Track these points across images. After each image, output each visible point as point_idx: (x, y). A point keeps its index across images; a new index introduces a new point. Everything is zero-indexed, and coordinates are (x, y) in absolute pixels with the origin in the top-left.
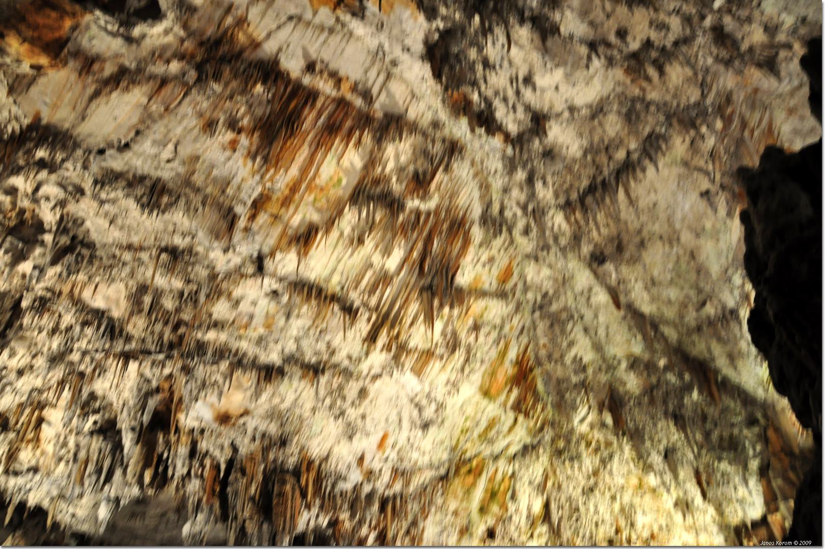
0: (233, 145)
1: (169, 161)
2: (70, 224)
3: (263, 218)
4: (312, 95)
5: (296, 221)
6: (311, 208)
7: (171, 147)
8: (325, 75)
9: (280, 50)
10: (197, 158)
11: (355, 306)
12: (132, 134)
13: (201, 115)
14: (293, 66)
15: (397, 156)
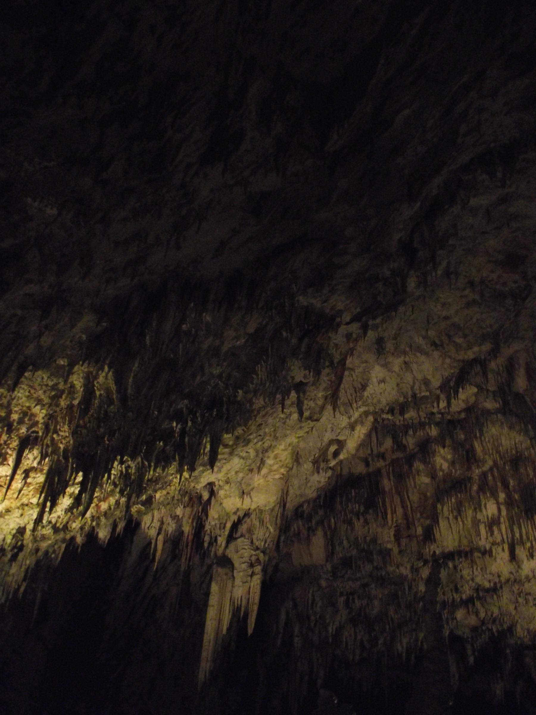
0: (366, 522)
1: (350, 546)
2: (342, 590)
3: (404, 541)
4: (378, 472)
5: (420, 530)
6: (422, 520)
7: (345, 542)
8: (376, 459)
9: (350, 468)
10: (358, 538)
11: (488, 549)
12: (330, 548)
13: (344, 522)
14: (360, 469)
15: (444, 458)
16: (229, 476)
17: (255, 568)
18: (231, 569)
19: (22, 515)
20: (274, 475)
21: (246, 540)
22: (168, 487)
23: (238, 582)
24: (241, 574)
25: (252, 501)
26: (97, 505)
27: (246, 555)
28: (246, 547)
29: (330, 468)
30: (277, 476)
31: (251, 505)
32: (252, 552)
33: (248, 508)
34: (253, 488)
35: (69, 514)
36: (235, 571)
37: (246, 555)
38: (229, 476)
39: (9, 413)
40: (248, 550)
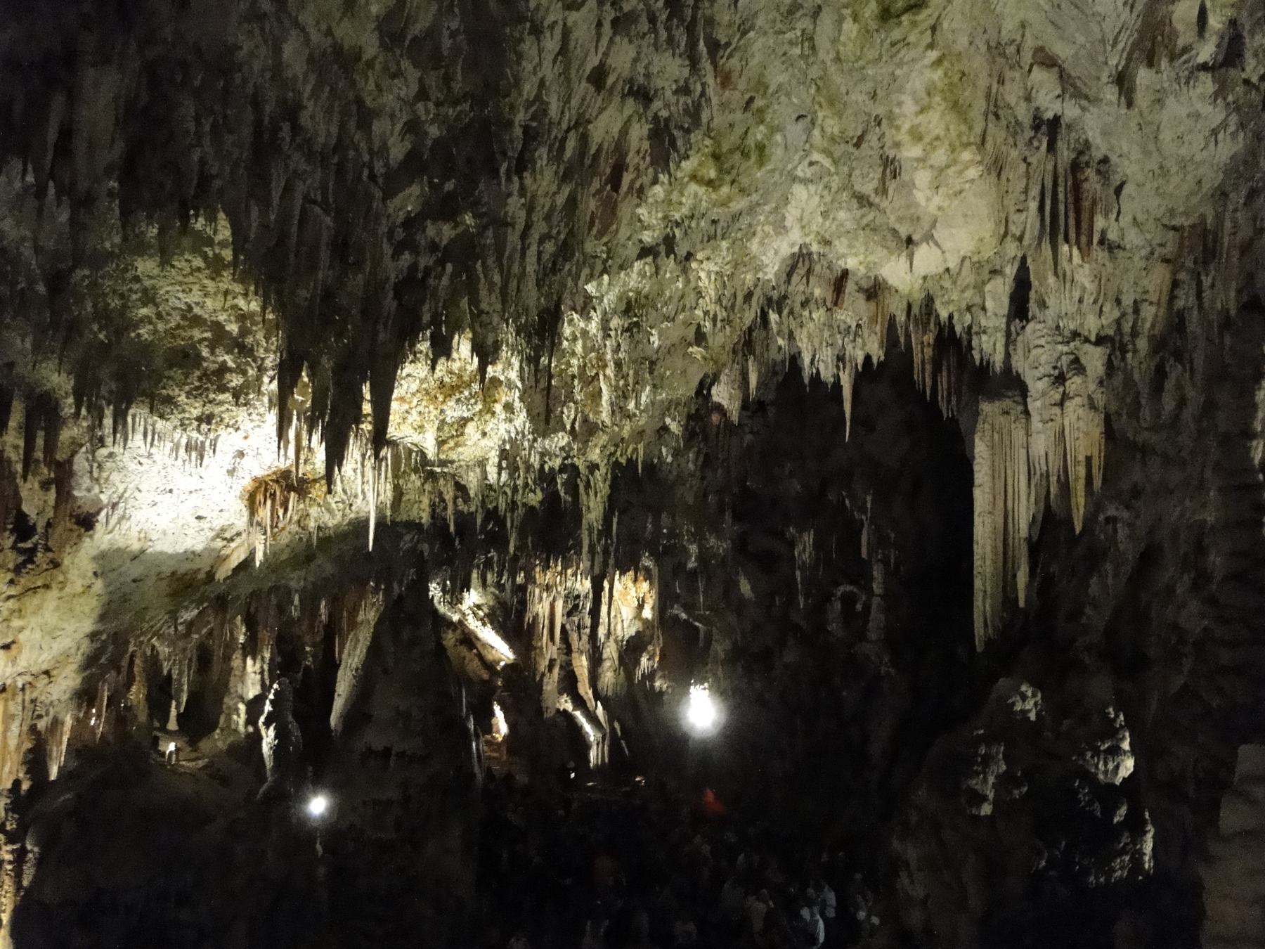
16: (814, 228)
17: (1067, 384)
18: (1019, 399)
19: (484, 434)
20: (961, 172)
21: (1039, 326)
22: (701, 301)
23: (1036, 423)
24: (1038, 404)
25: (943, 252)
26: (605, 375)
27: (1043, 359)
28: (1042, 341)
29: (1204, 67)
30: (973, 173)
31: (945, 261)
32: (1060, 347)
33: (941, 270)
34: (934, 224)
35: (571, 404)
36: (1029, 400)
37: (1043, 359)
38: (814, 228)
39: (217, 327)
40: (1048, 347)
